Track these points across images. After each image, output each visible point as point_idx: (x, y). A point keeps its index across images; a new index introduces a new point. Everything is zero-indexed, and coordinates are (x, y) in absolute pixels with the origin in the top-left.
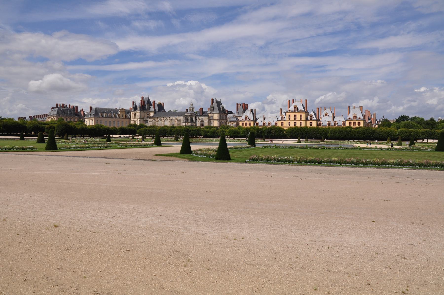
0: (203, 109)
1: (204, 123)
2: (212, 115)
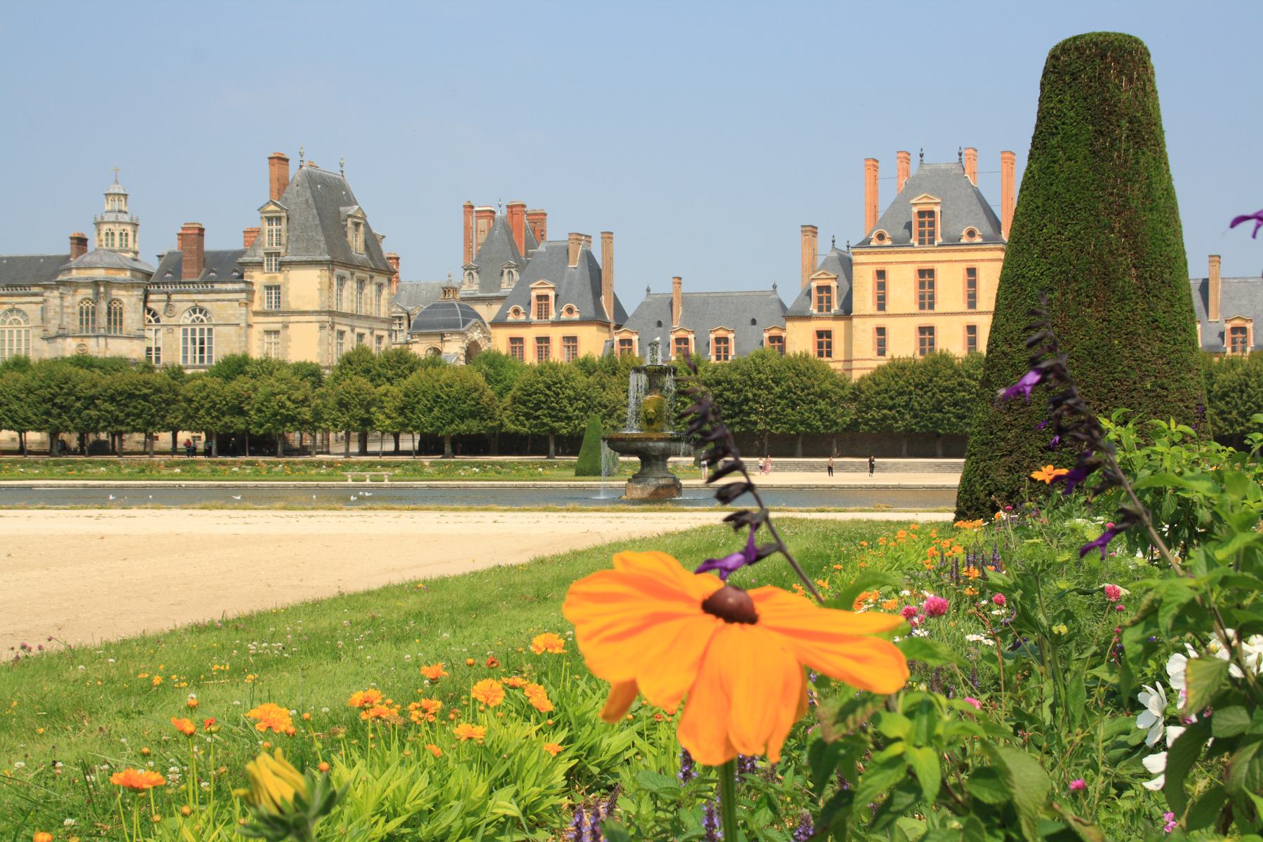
0: (201, 230)
1: (210, 339)
2: (280, 278)
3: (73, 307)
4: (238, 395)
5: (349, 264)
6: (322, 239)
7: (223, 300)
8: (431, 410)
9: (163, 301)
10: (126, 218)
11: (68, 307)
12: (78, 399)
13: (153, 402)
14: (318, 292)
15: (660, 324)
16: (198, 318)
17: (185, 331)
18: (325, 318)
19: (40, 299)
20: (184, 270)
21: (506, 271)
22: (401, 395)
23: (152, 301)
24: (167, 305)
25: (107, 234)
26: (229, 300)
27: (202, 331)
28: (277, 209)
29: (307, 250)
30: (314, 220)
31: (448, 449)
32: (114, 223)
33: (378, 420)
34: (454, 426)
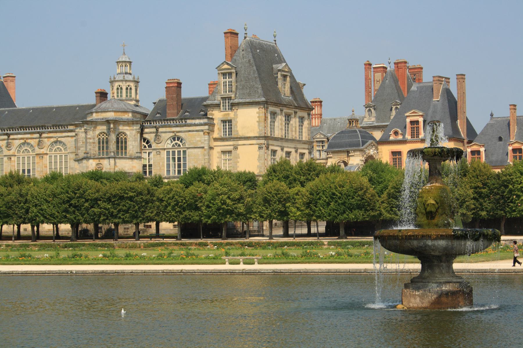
0: (179, 84)
1: (185, 158)
2: (231, 115)
3: (94, 139)
4: (194, 196)
5: (279, 104)
6: (260, 86)
7: (193, 131)
8: (328, 204)
9: (154, 133)
10: (130, 78)
11: (90, 139)
12: (87, 201)
13: (136, 202)
14: (257, 124)
15: (500, 139)
16: (176, 144)
17: (168, 153)
18: (262, 141)
19: (73, 134)
20: (168, 111)
21: (394, 107)
22: (308, 194)
23: (147, 133)
24: (156, 136)
25: (118, 89)
27: (179, 152)
28: (229, 67)
29: (249, 95)
30: (254, 73)
31: (342, 232)
32: (122, 81)
33: (291, 212)
34: (345, 215)
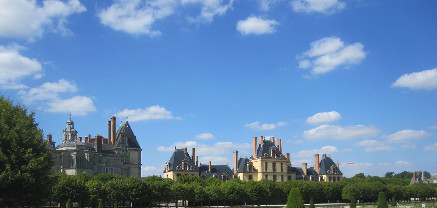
14: (138, 159)
16: (108, 165)
26: (119, 159)
